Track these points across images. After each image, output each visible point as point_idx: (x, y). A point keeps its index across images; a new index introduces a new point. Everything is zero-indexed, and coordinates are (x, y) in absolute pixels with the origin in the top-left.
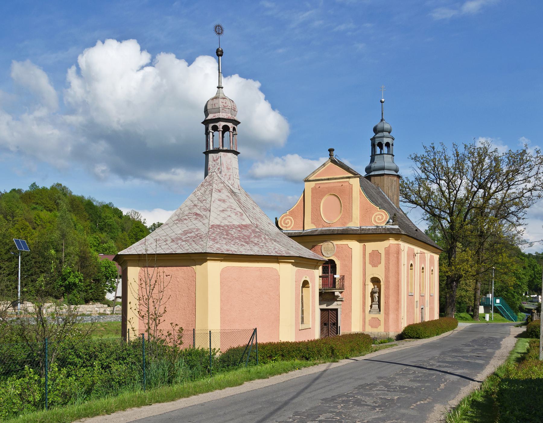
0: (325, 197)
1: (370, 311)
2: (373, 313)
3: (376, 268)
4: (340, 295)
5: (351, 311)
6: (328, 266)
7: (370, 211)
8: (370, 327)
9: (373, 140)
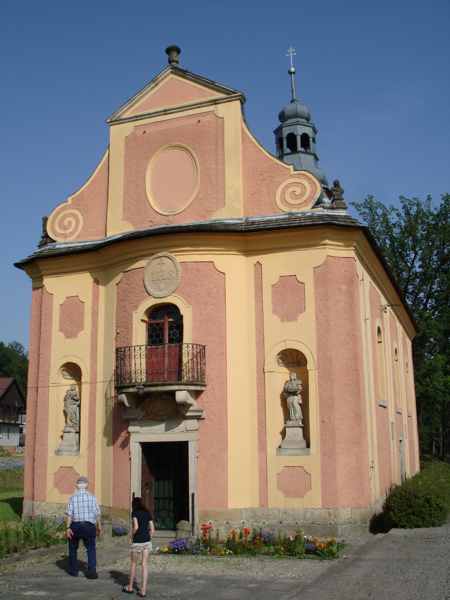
0: (157, 154)
1: (280, 447)
2: (290, 452)
3: (293, 323)
4: (190, 400)
5: (225, 449)
6: (163, 324)
7: (270, 177)
8: (280, 495)
9: (278, 131)
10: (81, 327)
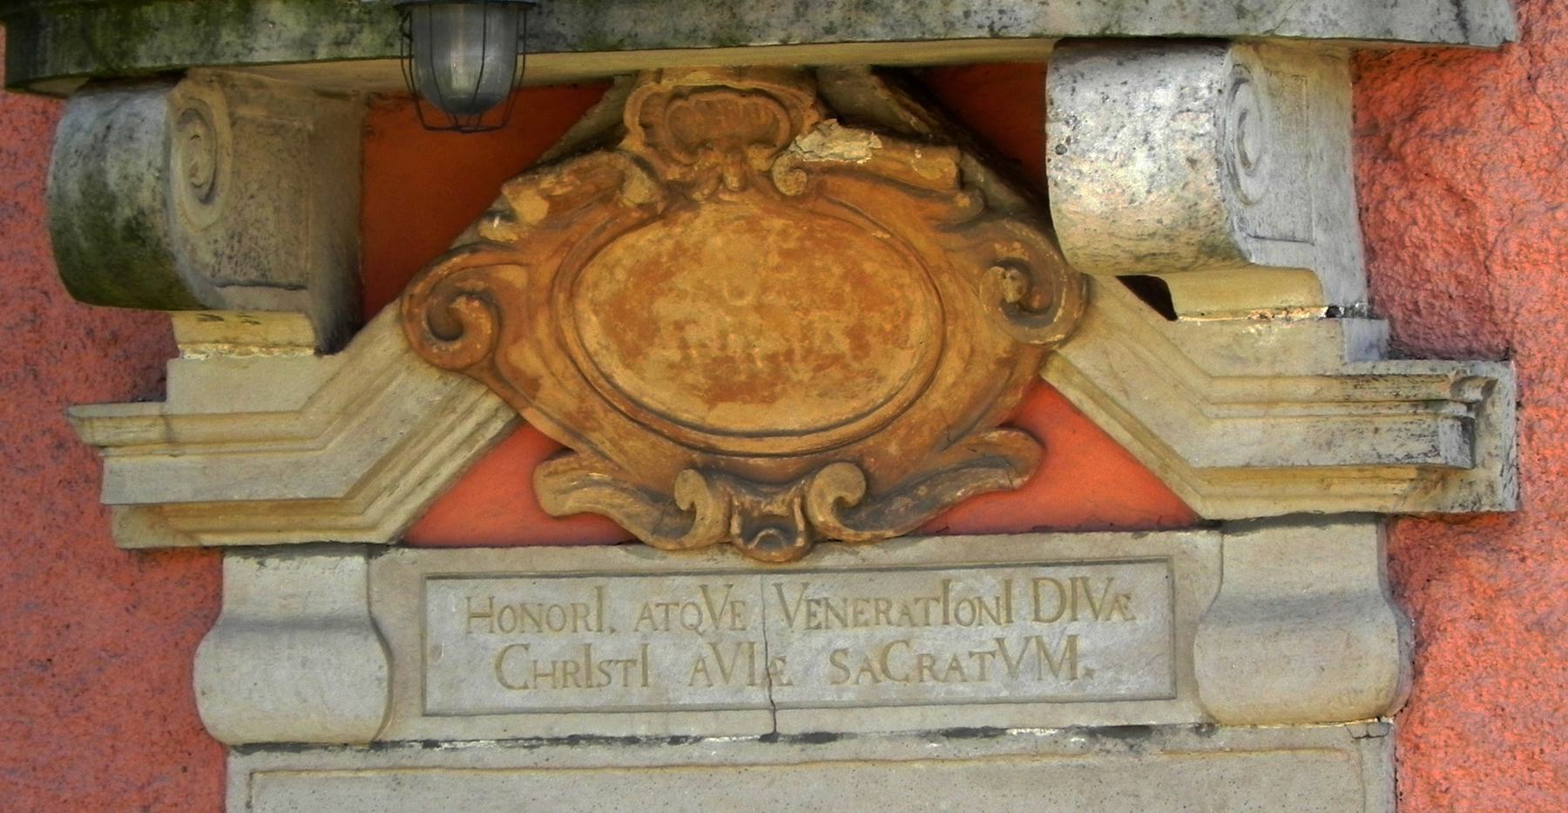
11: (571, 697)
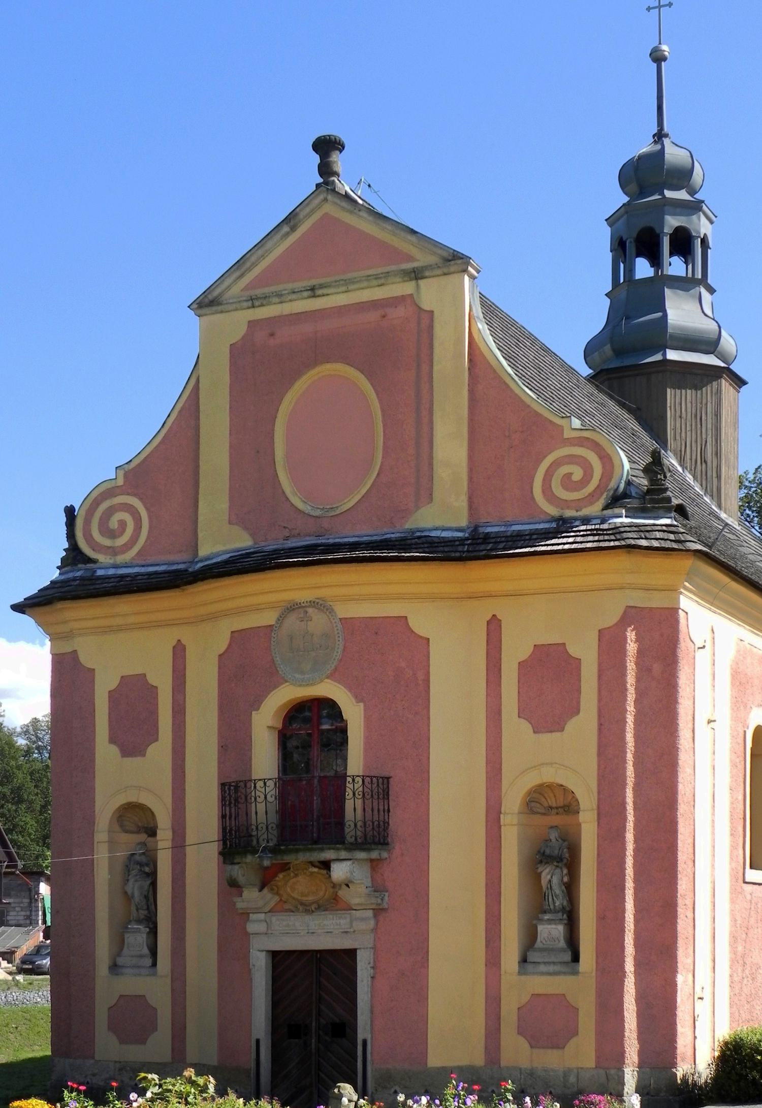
10: (153, 735)
11: (286, 928)
